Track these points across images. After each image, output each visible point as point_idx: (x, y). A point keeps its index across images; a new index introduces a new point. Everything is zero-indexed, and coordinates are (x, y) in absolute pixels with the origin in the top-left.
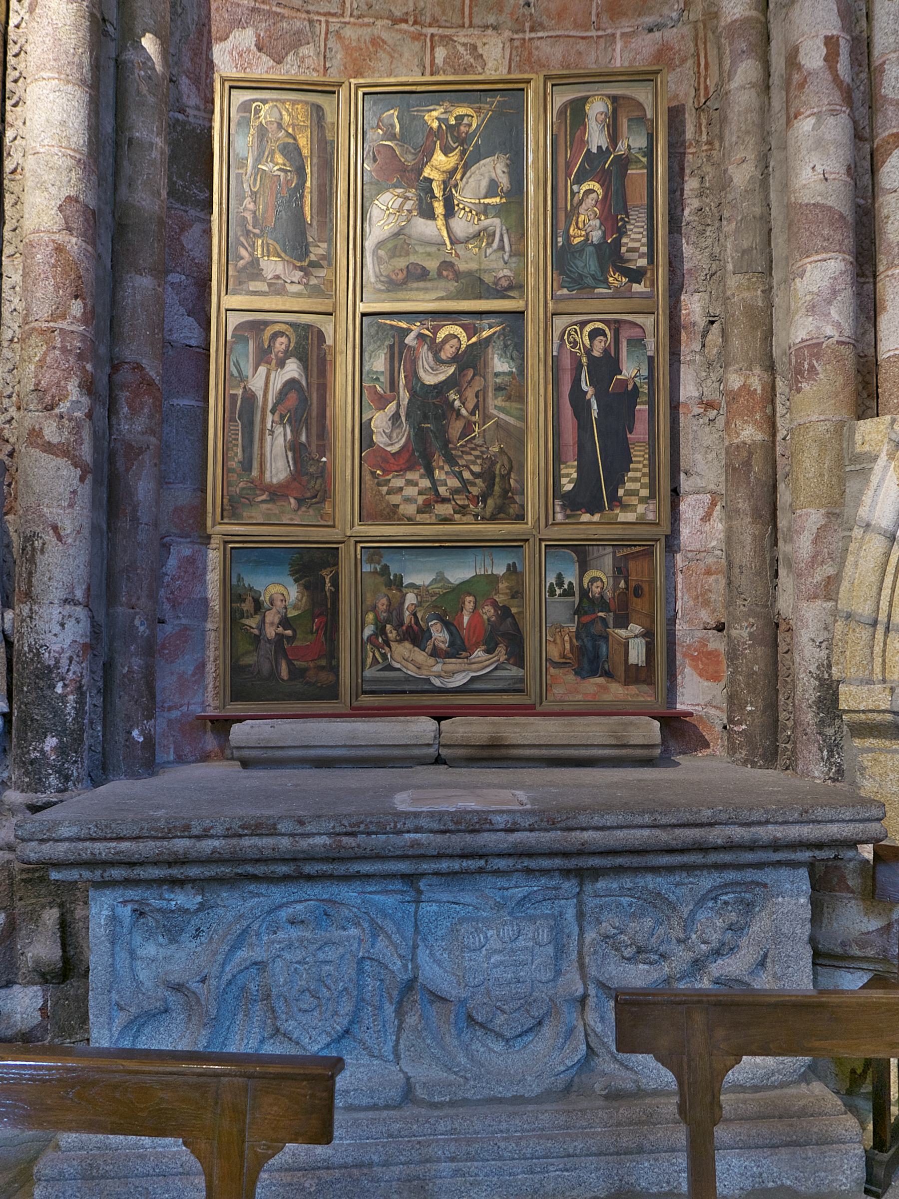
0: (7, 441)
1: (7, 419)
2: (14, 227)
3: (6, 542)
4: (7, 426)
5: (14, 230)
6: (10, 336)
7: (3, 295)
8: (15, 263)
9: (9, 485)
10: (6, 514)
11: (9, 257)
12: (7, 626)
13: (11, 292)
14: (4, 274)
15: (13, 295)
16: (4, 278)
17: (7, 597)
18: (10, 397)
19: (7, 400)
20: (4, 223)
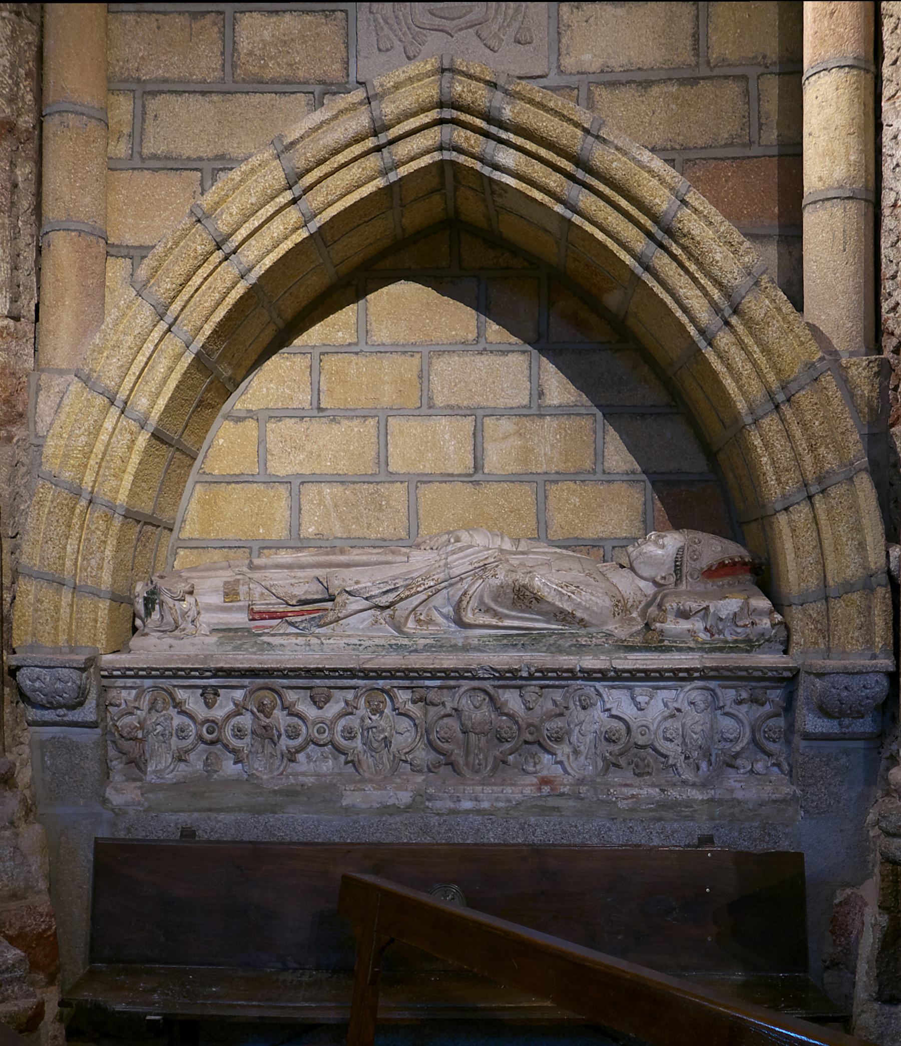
0: (892, 334)
1: (892, 305)
2: (894, 58)
3: (892, 460)
4: (892, 315)
5: (895, 63)
6: (893, 200)
7: (884, 150)
8: (897, 105)
9: (896, 389)
10: (892, 425)
11: (889, 99)
12: (892, 566)
13: (892, 144)
14: (885, 124)
15: (895, 147)
16: (885, 128)
17: (895, 530)
18: (894, 277)
19: (891, 282)
20: (884, 58)
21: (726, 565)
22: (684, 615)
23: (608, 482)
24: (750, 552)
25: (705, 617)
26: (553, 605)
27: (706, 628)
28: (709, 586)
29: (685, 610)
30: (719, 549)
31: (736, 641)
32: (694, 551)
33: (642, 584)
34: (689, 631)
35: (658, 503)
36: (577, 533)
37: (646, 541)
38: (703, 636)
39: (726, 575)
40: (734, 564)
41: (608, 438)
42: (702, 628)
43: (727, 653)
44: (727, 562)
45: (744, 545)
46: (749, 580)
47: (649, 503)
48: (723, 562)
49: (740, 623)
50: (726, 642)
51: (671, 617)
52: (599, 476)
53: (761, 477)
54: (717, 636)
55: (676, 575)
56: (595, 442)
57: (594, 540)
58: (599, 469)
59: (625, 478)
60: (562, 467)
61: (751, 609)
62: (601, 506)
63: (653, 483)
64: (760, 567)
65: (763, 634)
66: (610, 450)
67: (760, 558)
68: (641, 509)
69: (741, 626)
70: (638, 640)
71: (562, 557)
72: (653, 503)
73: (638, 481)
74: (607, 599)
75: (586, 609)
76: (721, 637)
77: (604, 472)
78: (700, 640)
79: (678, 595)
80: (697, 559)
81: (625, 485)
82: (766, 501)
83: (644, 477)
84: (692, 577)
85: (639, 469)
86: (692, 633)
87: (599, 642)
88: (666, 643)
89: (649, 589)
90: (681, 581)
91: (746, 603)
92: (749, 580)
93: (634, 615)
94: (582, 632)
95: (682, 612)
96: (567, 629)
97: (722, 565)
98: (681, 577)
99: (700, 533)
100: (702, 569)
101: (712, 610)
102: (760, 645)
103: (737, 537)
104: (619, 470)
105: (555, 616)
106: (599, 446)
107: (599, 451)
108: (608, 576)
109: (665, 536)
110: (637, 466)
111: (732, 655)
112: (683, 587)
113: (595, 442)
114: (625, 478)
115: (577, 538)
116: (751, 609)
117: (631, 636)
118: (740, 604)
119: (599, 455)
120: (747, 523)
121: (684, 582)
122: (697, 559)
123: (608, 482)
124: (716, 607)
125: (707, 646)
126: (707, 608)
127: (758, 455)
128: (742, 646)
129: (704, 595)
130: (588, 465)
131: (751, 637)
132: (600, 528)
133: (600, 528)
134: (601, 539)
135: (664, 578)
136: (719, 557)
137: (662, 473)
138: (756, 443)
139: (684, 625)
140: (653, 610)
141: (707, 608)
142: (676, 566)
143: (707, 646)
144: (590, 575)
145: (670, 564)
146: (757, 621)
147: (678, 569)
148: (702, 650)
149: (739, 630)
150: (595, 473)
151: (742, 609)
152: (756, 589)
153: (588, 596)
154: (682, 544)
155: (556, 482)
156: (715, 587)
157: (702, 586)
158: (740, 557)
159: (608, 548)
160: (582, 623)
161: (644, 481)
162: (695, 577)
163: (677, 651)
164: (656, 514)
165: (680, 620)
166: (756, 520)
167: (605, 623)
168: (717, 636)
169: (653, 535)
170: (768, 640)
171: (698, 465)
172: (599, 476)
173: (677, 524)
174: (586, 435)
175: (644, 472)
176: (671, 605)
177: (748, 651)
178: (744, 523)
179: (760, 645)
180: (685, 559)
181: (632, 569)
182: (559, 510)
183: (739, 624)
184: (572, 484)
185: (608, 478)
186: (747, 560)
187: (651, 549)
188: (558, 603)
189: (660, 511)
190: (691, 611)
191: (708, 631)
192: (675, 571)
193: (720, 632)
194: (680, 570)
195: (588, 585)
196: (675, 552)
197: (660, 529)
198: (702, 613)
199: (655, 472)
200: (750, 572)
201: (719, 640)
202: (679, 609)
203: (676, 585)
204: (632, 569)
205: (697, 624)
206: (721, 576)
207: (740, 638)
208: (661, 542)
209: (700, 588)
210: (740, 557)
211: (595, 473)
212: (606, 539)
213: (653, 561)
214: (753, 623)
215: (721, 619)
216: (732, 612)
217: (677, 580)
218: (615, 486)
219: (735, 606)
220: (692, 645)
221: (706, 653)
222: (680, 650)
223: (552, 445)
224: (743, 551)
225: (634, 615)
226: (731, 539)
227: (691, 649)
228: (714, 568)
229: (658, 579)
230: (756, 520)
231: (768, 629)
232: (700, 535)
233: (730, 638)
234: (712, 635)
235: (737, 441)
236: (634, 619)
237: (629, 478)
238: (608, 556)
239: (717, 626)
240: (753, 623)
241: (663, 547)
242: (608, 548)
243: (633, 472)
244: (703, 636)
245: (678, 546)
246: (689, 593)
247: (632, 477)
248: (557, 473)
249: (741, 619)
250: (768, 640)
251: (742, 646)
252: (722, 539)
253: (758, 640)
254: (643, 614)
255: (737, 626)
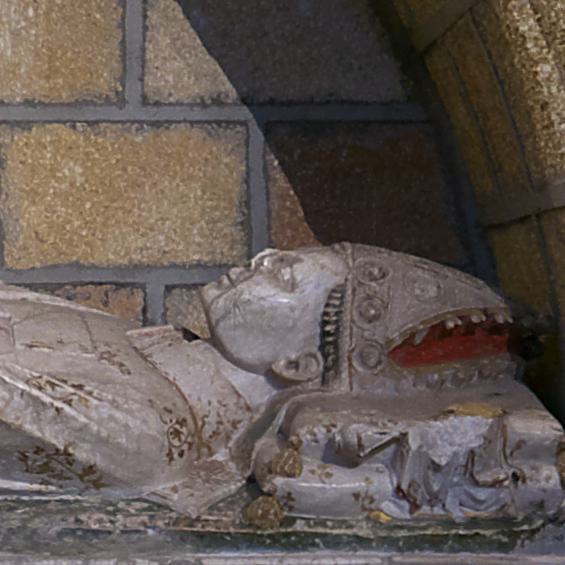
21: (450, 332)
22: (345, 456)
23: (156, 124)
24: (508, 299)
25: (396, 462)
26: (19, 430)
27: (398, 489)
28: (407, 384)
29: (347, 445)
30: (432, 292)
31: (473, 522)
32: (369, 297)
33: (240, 379)
34: (356, 496)
35: (281, 180)
36: (79, 254)
37: (250, 272)
38: (392, 510)
39: (449, 357)
40: (470, 329)
41: (154, 17)
42: (390, 488)
43: (453, 550)
44: (451, 325)
45: (494, 282)
46: (508, 370)
47: (257, 178)
48: (443, 324)
49: (485, 477)
50: (450, 523)
51: (311, 462)
52: (133, 111)
53: (537, 114)
54: (426, 509)
55: (325, 356)
56: (122, 26)
57: (119, 269)
58: (133, 94)
59: (198, 114)
60: (40, 88)
61: (512, 439)
62: (137, 185)
63: (267, 129)
64: (533, 338)
65: (541, 505)
66: (160, 45)
67: (534, 314)
68: (237, 191)
69: (486, 485)
70: (229, 519)
71: (40, 313)
72: (267, 178)
73: (228, 123)
74: (153, 417)
75: (100, 441)
76: (438, 510)
77: (145, 101)
78: (384, 518)
79: (329, 406)
80: (376, 317)
81: (197, 133)
82: (549, 172)
83: (245, 113)
84: (364, 363)
85: (233, 94)
86: (364, 501)
87: (132, 523)
88: (299, 526)
89: (258, 392)
90: (338, 373)
91: (499, 426)
92: (508, 370)
93: (221, 456)
94: (91, 498)
95: (339, 451)
96: (54, 492)
97: (438, 331)
98: (336, 361)
99: (385, 253)
100: (389, 341)
101: (413, 443)
102: (533, 532)
103: (475, 259)
104: (182, 96)
105: (24, 458)
106: (134, 36)
107: (133, 47)
108: (157, 358)
109: (298, 260)
110: (229, 86)
111: (464, 556)
112: (341, 387)
113: (122, 26)
114: (198, 114)
115: (77, 265)
116: (512, 439)
117: (213, 508)
118: (484, 430)
119: (132, 59)
120: (502, 226)
121: (345, 375)
122: (376, 317)
123: (156, 124)
124: (423, 436)
125: (402, 533)
126: (401, 440)
127: (530, 58)
128: (488, 533)
129: (394, 407)
130: (105, 82)
131: (512, 511)
132: (135, 241)
133: (135, 241)
134: (138, 267)
135: (294, 364)
136: (432, 312)
137: (290, 103)
138: (523, 28)
139: (345, 482)
140: (267, 445)
141: (401, 440)
142: (325, 334)
143: (402, 533)
144: (108, 357)
145: (308, 331)
146: (527, 472)
147: (328, 341)
148: (390, 543)
149: (482, 494)
150: (121, 101)
151: (488, 440)
152: (524, 390)
153: (105, 410)
154: (339, 280)
155: (26, 125)
156: (422, 388)
157: (389, 383)
158: (485, 312)
159: (156, 289)
160: (91, 476)
161: (244, 123)
162: (373, 361)
163: (328, 545)
164: (275, 204)
165: (333, 469)
166: (524, 220)
167: (148, 477)
168: (426, 509)
169: (266, 257)
170: (553, 520)
171: (383, 83)
172: (133, 111)
173: (327, 232)
174: (100, 9)
175: (245, 100)
176: (312, 430)
177: (503, 548)
178: (493, 227)
179: (533, 532)
180: (346, 317)
181: (215, 341)
182: (33, 195)
183: (481, 478)
184: (64, 131)
185: (156, 116)
186: (500, 320)
187: (261, 292)
188: (30, 428)
189: (283, 197)
190: (361, 446)
191: (405, 497)
192: (322, 348)
193: (434, 499)
194: (335, 344)
195: (105, 382)
196: (323, 300)
197: (286, 242)
198: (390, 450)
199: (272, 102)
200: (509, 349)
201: (433, 517)
202: (331, 441)
203: (324, 381)
204: (215, 341)
205: (375, 478)
206: (435, 360)
207: (483, 514)
208: (286, 274)
209: (383, 388)
210: (485, 312)
211: (121, 101)
212: (149, 268)
213: (265, 323)
214: (515, 477)
215: (436, 468)
216: (463, 450)
217: (327, 369)
218: (174, 135)
219: (471, 435)
220: (364, 531)
221: (400, 550)
222: (333, 543)
223: (15, 34)
224: (493, 299)
225: (221, 456)
226: (462, 268)
227: (361, 542)
228: (418, 340)
229: (280, 366)
230: (524, 220)
231: (553, 492)
232: (383, 257)
233: (458, 514)
234: (415, 507)
235: (477, 24)
236: (218, 467)
237: (208, 116)
238: (156, 312)
239: (427, 484)
240: (515, 477)
241: (292, 286)
242: (156, 289)
243: (218, 101)
244: (392, 510)
245: (330, 285)
246: (357, 403)
247: (214, 113)
248: (28, 103)
249: (486, 467)
250: (553, 520)
251: (488, 533)
252: (438, 267)
253: (528, 520)
254: (243, 454)
255: (477, 484)
